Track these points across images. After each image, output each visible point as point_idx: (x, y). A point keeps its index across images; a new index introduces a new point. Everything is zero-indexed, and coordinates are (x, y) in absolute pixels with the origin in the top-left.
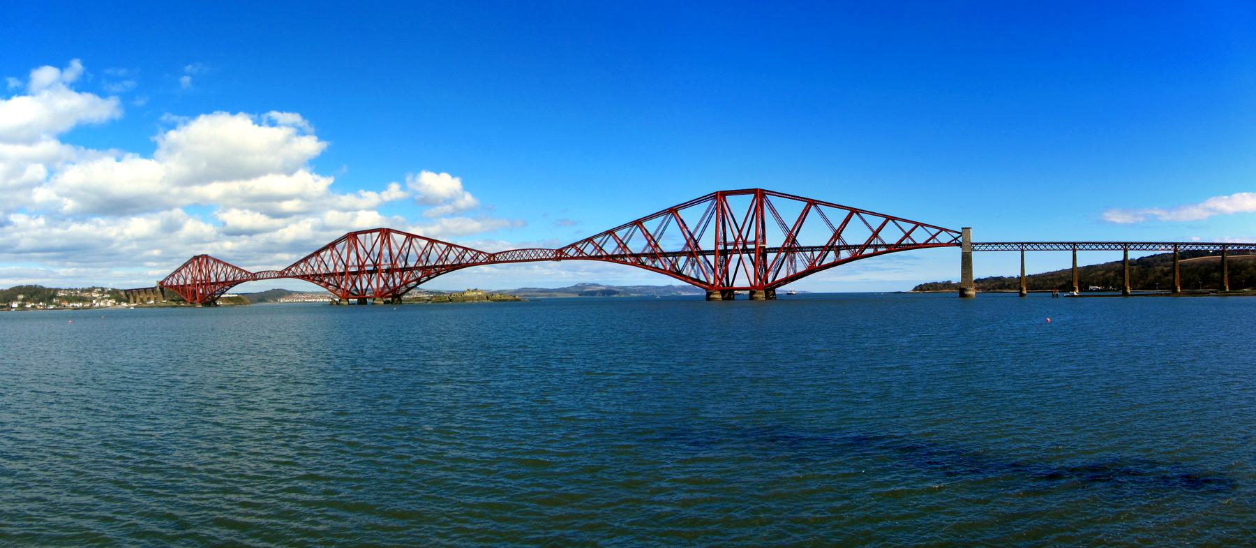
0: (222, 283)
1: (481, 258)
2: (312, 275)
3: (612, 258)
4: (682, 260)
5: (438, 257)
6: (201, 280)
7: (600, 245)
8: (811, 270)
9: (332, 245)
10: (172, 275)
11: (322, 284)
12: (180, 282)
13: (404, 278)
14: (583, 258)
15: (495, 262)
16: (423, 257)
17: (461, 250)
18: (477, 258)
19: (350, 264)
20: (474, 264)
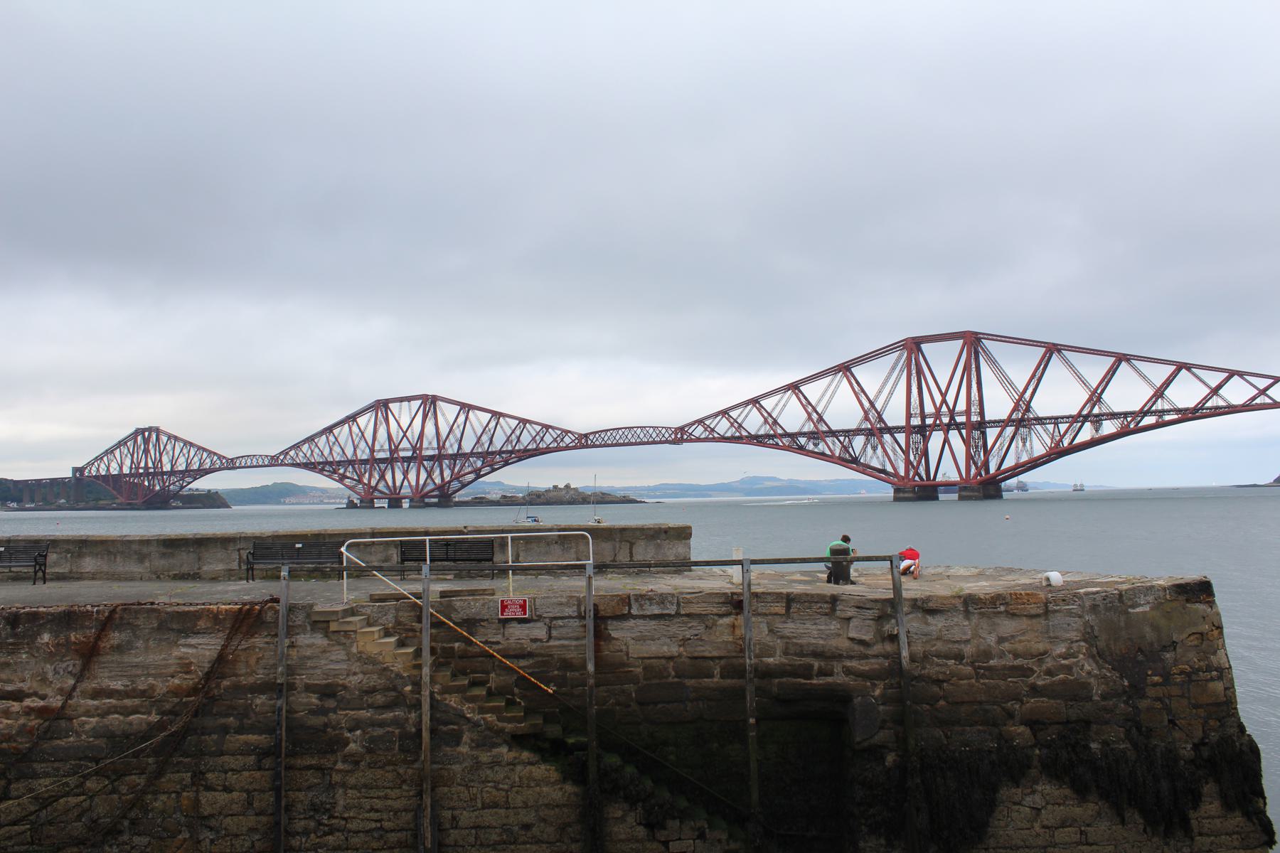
0: (181, 472)
1: (567, 440)
2: (320, 463)
3: (757, 440)
4: (859, 442)
6: (146, 467)
7: (739, 421)
8: (1057, 453)
9: (352, 418)
10: (99, 458)
11: (336, 476)
12: (111, 470)
13: (456, 470)
14: (714, 440)
15: (587, 446)
16: (485, 438)
17: (538, 428)
18: (562, 440)
19: (377, 447)
20: (558, 449)
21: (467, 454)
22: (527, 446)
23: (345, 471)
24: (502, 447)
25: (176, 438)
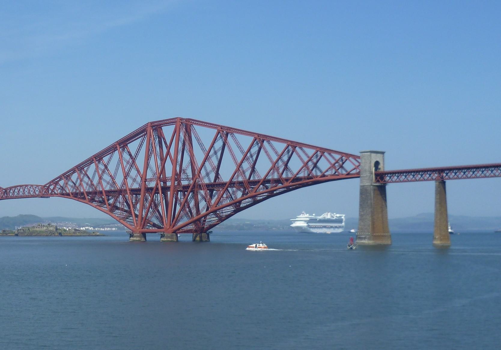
2: (88, 193)
5: (270, 165)
11: (106, 208)
20: (336, 178)
21: (225, 184)
22: (297, 174)
23: (116, 201)
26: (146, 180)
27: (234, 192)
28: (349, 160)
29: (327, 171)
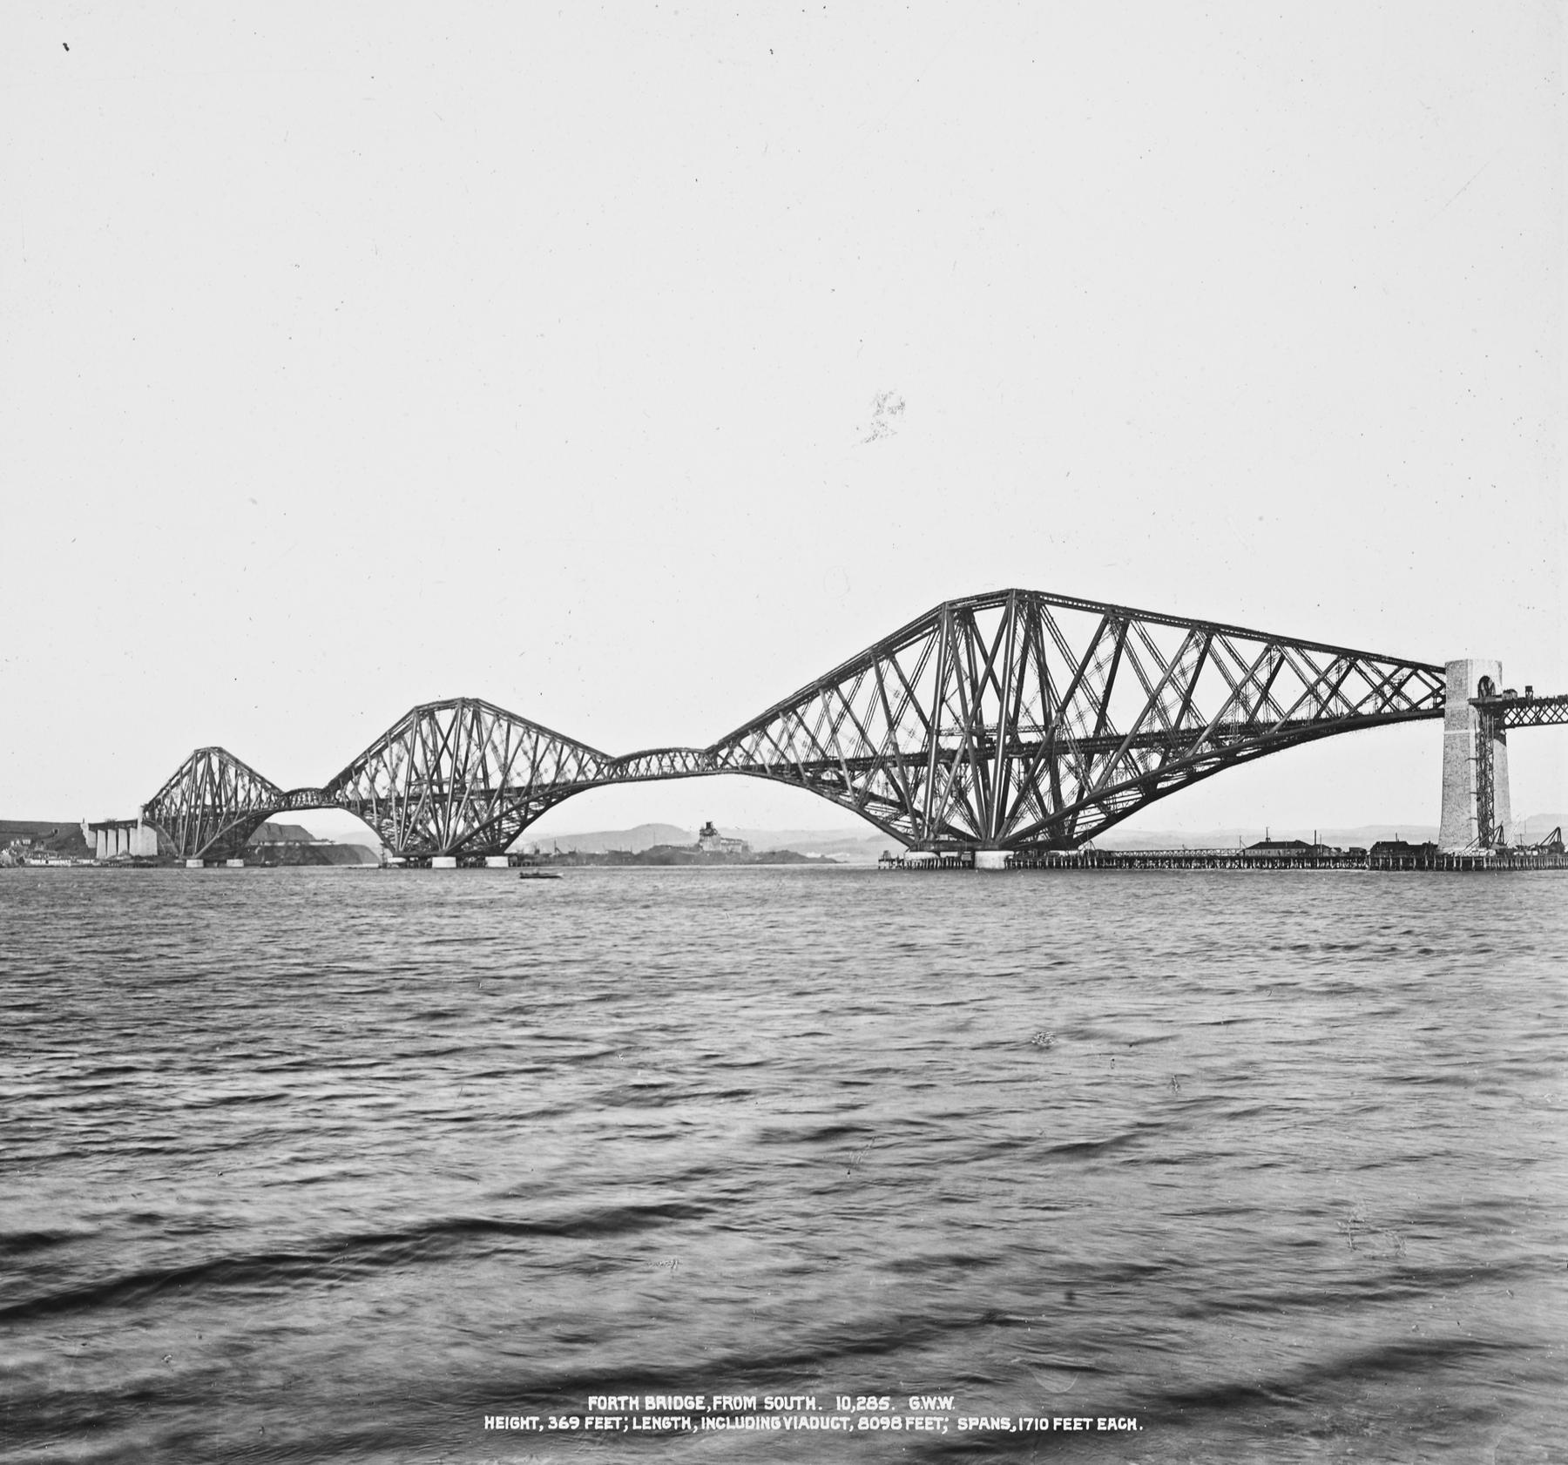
0: (519, 789)
2: (807, 765)
17: (1323, 660)
18: (1397, 691)
23: (869, 780)
24: (1222, 713)
25: (512, 718)
26: (939, 733)
27: (1142, 757)
28: (1418, 676)
29: (1363, 702)
